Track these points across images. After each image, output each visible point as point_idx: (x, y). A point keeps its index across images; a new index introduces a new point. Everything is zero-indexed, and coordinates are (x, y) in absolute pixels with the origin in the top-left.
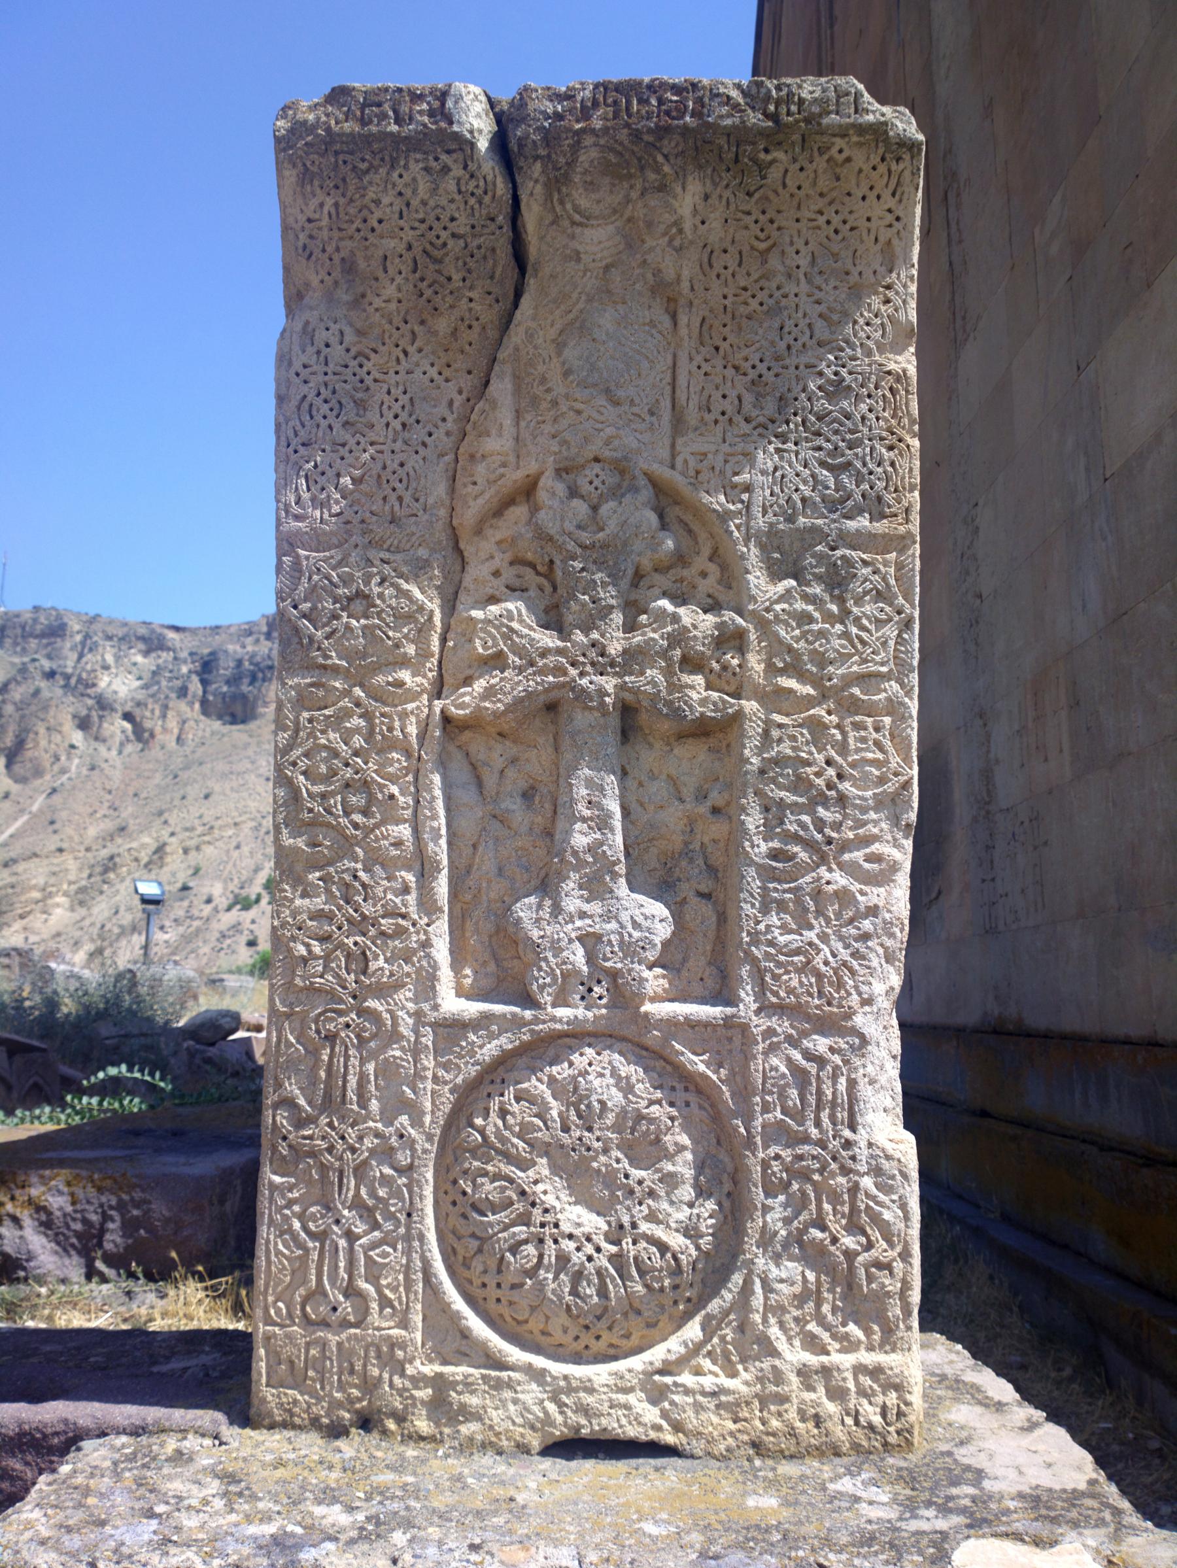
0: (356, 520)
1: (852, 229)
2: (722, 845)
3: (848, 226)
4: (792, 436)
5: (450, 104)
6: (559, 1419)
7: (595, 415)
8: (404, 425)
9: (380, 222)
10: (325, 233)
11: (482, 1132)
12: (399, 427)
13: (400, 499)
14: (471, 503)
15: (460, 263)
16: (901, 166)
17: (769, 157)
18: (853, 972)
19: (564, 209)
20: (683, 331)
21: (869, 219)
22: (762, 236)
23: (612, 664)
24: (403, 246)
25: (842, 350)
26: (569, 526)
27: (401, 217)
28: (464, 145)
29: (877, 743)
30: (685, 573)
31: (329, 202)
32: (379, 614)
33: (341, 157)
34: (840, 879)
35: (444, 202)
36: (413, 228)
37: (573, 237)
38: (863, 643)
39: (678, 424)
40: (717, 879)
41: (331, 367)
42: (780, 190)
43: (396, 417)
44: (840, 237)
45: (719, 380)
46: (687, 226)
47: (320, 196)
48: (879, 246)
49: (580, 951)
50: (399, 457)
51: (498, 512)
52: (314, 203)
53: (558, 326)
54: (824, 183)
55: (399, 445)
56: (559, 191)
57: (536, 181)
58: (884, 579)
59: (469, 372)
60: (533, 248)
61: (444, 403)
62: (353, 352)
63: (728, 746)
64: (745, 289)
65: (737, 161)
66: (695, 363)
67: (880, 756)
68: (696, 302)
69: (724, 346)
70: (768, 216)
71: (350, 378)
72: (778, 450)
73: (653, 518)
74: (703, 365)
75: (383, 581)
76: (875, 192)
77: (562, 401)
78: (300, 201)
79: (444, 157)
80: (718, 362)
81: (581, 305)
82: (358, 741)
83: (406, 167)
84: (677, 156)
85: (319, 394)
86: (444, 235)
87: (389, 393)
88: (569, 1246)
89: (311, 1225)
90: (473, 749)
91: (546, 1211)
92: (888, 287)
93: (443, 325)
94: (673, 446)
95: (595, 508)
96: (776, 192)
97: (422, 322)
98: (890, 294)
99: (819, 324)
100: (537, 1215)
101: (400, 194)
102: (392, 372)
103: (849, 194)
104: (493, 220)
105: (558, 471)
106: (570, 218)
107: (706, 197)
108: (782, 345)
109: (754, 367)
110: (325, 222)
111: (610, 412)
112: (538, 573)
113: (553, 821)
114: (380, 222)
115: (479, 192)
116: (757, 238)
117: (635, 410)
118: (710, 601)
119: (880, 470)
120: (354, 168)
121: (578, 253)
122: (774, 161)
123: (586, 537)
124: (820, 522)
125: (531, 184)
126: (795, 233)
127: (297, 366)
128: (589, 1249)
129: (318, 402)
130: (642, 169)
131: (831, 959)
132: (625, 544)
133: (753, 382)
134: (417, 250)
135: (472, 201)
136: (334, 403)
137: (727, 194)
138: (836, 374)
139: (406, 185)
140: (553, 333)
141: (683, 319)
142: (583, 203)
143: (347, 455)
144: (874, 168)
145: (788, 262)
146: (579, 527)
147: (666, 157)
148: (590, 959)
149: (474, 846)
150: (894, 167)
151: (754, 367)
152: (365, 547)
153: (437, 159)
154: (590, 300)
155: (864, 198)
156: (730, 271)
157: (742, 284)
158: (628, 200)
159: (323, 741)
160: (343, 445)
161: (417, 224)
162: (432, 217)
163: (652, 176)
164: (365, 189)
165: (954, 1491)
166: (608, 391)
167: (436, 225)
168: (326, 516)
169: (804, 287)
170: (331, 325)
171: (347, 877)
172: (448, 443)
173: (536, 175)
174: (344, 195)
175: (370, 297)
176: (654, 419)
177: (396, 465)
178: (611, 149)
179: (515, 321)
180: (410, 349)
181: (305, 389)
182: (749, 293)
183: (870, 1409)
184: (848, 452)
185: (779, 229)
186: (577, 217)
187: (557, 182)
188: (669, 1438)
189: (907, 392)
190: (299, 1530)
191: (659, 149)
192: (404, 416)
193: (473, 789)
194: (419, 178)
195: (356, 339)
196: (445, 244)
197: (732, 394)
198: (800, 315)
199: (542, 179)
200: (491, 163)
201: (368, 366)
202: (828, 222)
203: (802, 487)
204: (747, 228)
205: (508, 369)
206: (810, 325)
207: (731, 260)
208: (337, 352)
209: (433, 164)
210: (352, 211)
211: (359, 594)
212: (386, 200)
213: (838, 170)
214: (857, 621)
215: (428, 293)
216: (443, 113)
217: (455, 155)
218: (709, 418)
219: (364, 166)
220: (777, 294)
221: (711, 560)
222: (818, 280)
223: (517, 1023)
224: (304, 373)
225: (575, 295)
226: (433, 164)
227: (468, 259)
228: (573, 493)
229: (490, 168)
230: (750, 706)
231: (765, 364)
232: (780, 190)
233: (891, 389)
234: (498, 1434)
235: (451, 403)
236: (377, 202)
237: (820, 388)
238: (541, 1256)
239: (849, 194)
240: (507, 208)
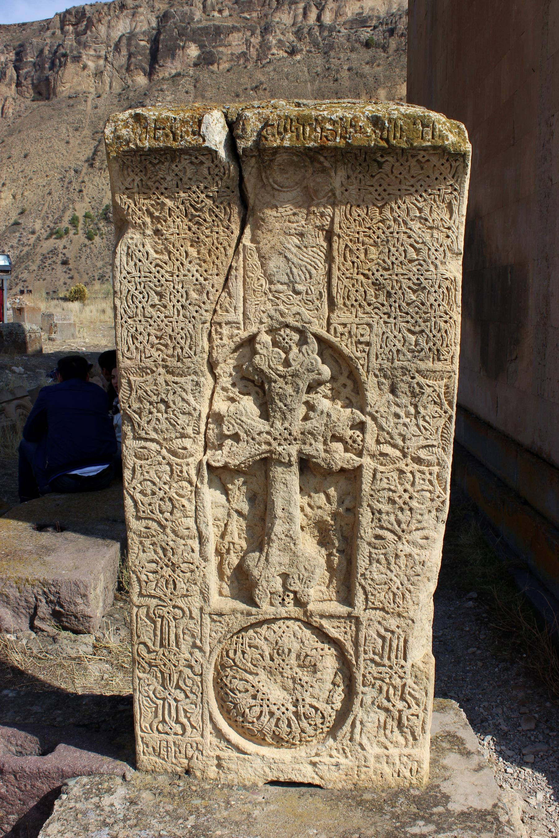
2: (350, 526)
4: (393, 315)
5: (203, 128)
6: (270, 774)
11: (234, 660)
16: (458, 164)
17: (383, 160)
18: (410, 592)
19: (269, 181)
22: (379, 198)
23: (295, 439)
25: (422, 265)
27: (177, 187)
28: (212, 153)
29: (430, 481)
31: (137, 179)
32: (173, 411)
33: (143, 158)
34: (407, 549)
37: (273, 196)
38: (426, 429)
40: (347, 543)
43: (178, 301)
49: (279, 580)
52: (129, 179)
56: (266, 173)
57: (253, 167)
58: (439, 396)
63: (355, 477)
67: (431, 488)
72: (385, 322)
75: (174, 393)
82: (166, 477)
83: (180, 162)
84: (332, 156)
88: (274, 708)
90: (223, 477)
91: (264, 694)
92: (449, 228)
96: (387, 175)
98: (450, 233)
100: (260, 696)
101: (177, 175)
103: (428, 177)
106: (271, 185)
107: (348, 177)
112: (255, 385)
113: (265, 513)
116: (376, 199)
119: (439, 335)
120: (151, 162)
122: (387, 161)
124: (405, 363)
125: (250, 169)
128: (283, 709)
131: (400, 586)
135: (217, 178)
137: (361, 176)
138: (418, 279)
139: (180, 171)
142: (279, 179)
147: (325, 157)
148: (284, 585)
149: (226, 525)
150: (454, 164)
158: (304, 177)
159: (148, 478)
160: (151, 318)
163: (318, 165)
164: (157, 172)
168: (143, 358)
171: (164, 544)
173: (252, 165)
174: (146, 175)
186: (276, 186)
188: (317, 781)
189: (456, 290)
191: (321, 155)
194: (187, 167)
196: (202, 201)
199: (256, 166)
203: (397, 343)
204: (371, 193)
211: (162, 401)
212: (169, 178)
214: (424, 417)
216: (199, 135)
217: (207, 157)
219: (156, 161)
221: (348, 377)
223: (249, 614)
226: (195, 161)
230: (366, 461)
233: (447, 288)
234: (244, 779)
236: (164, 179)
237: (409, 288)
238: (261, 712)
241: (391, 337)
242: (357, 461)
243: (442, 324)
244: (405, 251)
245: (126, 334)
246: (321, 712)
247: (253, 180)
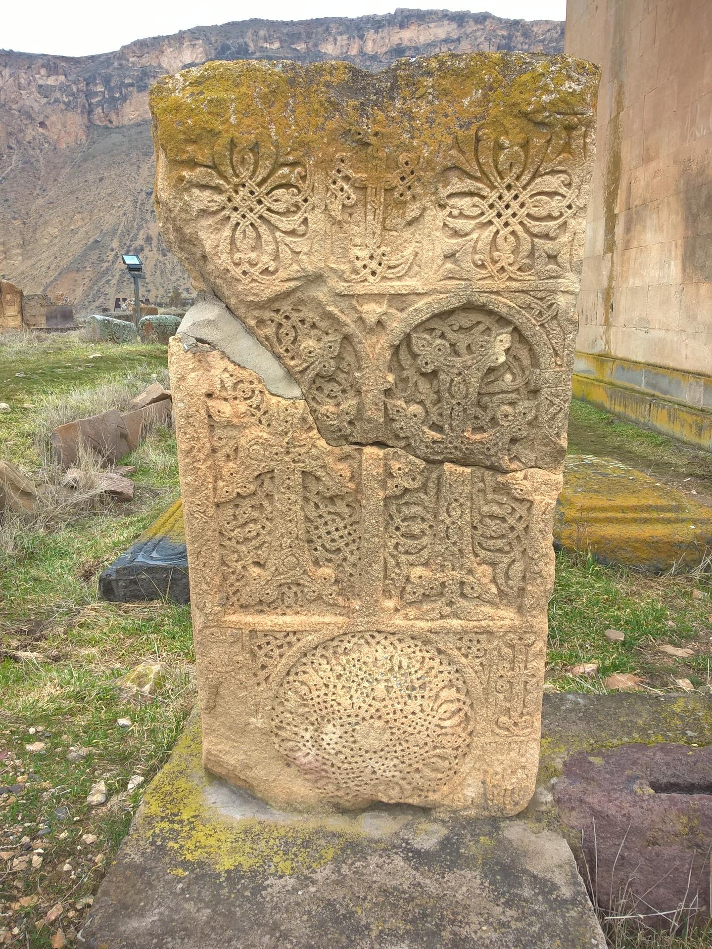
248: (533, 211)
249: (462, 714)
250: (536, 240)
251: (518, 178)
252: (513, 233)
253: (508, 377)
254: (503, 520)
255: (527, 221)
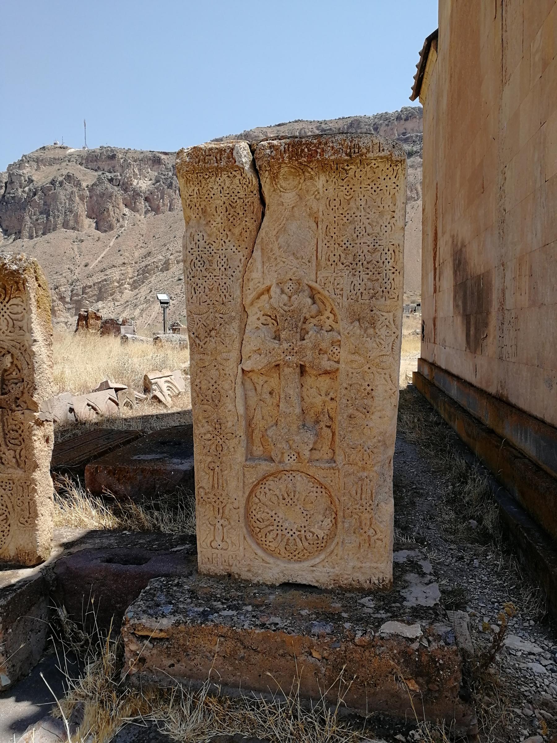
0: (211, 303)
1: (381, 190)
2: (334, 410)
3: (379, 189)
7: (290, 263)
8: (225, 269)
9: (214, 194)
10: (195, 200)
12: (224, 270)
13: (225, 296)
14: (248, 297)
15: (242, 208)
16: (398, 168)
20: (320, 231)
21: (387, 186)
22: (348, 194)
24: (222, 203)
26: (282, 305)
30: (322, 317)
31: (196, 189)
33: (199, 175)
35: (235, 187)
36: (225, 196)
37: (281, 196)
39: (318, 264)
41: (200, 249)
42: (354, 178)
44: (376, 193)
45: (333, 249)
46: (321, 192)
47: (193, 187)
48: (390, 196)
50: (224, 281)
51: (258, 298)
52: (191, 189)
53: (276, 230)
54: (370, 175)
55: (224, 277)
59: (246, 248)
60: (267, 201)
61: (238, 260)
62: (207, 243)
64: (342, 214)
65: (337, 169)
66: (324, 243)
68: (324, 220)
69: (334, 236)
70: (350, 187)
71: (207, 252)
73: (310, 301)
74: (327, 243)
76: (388, 177)
77: (278, 258)
78: (186, 189)
79: (234, 173)
80: (332, 242)
81: (284, 222)
85: (197, 259)
86: (236, 198)
87: (220, 257)
89: (211, 523)
90: (253, 378)
92: (394, 212)
93: (237, 231)
94: (317, 273)
95: (290, 297)
97: (230, 230)
99: (368, 227)
102: (220, 250)
103: (379, 178)
104: (252, 192)
105: (277, 284)
107: (327, 181)
108: (355, 235)
109: (345, 244)
110: (195, 196)
111: (295, 262)
112: (272, 319)
114: (214, 194)
115: (247, 183)
117: (303, 261)
118: (330, 328)
121: (283, 203)
122: (351, 168)
123: (286, 308)
126: (360, 193)
127: (189, 249)
129: (197, 261)
130: (303, 172)
132: (300, 310)
133: (345, 250)
134: (227, 204)
135: (245, 186)
136: (202, 262)
137: (335, 180)
140: (274, 233)
141: (320, 227)
142: (284, 185)
143: (207, 280)
144: (388, 169)
145: (357, 204)
146: (284, 305)
147: (312, 169)
150: (395, 168)
151: (345, 244)
152: (214, 313)
153: (231, 173)
154: (287, 220)
155: (384, 179)
156: (336, 207)
157: (341, 213)
160: (206, 277)
161: (226, 195)
162: (231, 192)
163: (307, 174)
165: (393, 605)
166: (294, 254)
167: (233, 195)
169: (363, 213)
170: (199, 233)
172: (240, 275)
173: (266, 176)
175: (212, 222)
176: (310, 264)
177: (223, 284)
178: (292, 168)
179: (262, 227)
180: (227, 241)
181: (192, 257)
182: (343, 216)
183: (374, 578)
184: (377, 275)
185: (354, 191)
186: (282, 189)
187: (274, 177)
190: (209, 610)
192: (225, 266)
193: (254, 391)
195: (208, 238)
196: (236, 201)
197: (337, 255)
198: (362, 223)
200: (251, 173)
201: (212, 247)
202: (372, 188)
205: (259, 247)
206: (365, 227)
207: (337, 204)
208: (202, 243)
209: (231, 175)
210: (204, 191)
212: (215, 188)
213: (374, 170)
215: (232, 219)
217: (237, 172)
218: (329, 263)
219: (207, 177)
220: (354, 216)
222: (368, 210)
224: (192, 251)
225: (282, 218)
226: (230, 175)
227: (245, 207)
228: (283, 292)
229: (250, 174)
231: (349, 243)
232: (354, 178)
235: (241, 260)
239: (379, 178)
240: (257, 188)
241: (357, 284)
242: (336, 365)
243: (391, 274)
244: (365, 227)
245: (190, 287)
246: (317, 536)
247: (267, 186)
248: (12, 311)
249: (4, 515)
250: (14, 321)
251: (4, 299)
252: (6, 319)
253: (14, 373)
254: (17, 432)
255: (10, 314)
